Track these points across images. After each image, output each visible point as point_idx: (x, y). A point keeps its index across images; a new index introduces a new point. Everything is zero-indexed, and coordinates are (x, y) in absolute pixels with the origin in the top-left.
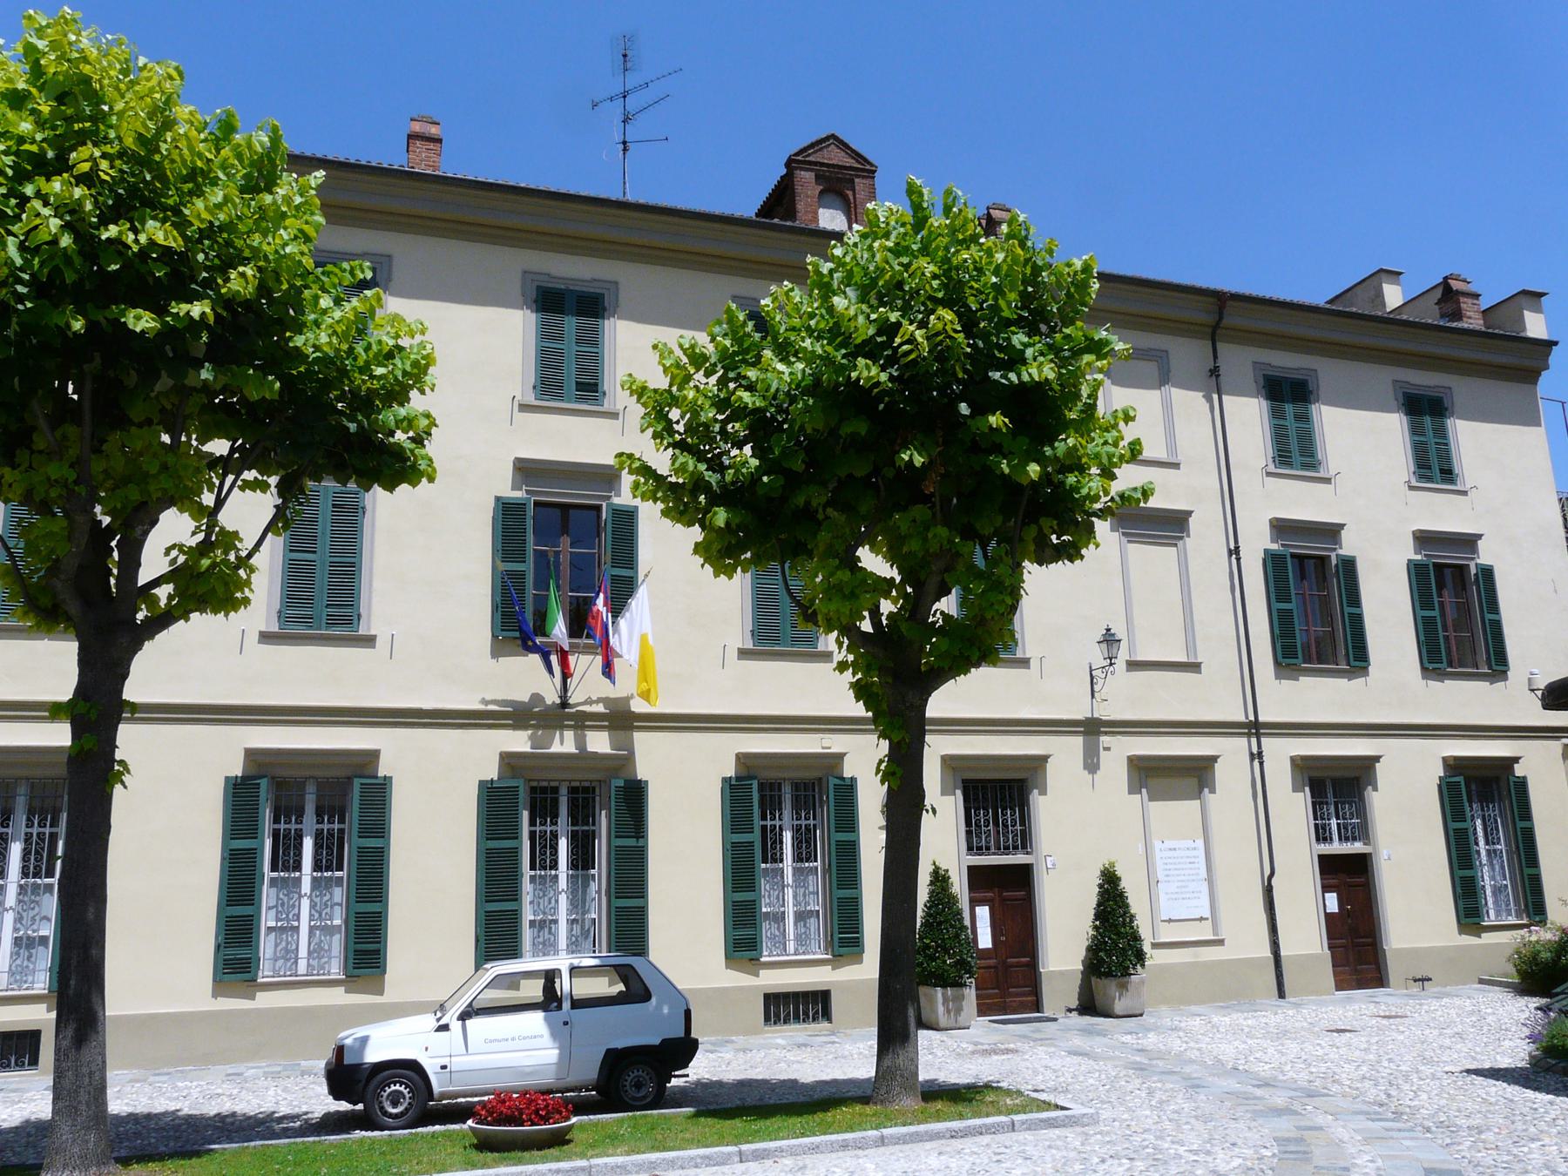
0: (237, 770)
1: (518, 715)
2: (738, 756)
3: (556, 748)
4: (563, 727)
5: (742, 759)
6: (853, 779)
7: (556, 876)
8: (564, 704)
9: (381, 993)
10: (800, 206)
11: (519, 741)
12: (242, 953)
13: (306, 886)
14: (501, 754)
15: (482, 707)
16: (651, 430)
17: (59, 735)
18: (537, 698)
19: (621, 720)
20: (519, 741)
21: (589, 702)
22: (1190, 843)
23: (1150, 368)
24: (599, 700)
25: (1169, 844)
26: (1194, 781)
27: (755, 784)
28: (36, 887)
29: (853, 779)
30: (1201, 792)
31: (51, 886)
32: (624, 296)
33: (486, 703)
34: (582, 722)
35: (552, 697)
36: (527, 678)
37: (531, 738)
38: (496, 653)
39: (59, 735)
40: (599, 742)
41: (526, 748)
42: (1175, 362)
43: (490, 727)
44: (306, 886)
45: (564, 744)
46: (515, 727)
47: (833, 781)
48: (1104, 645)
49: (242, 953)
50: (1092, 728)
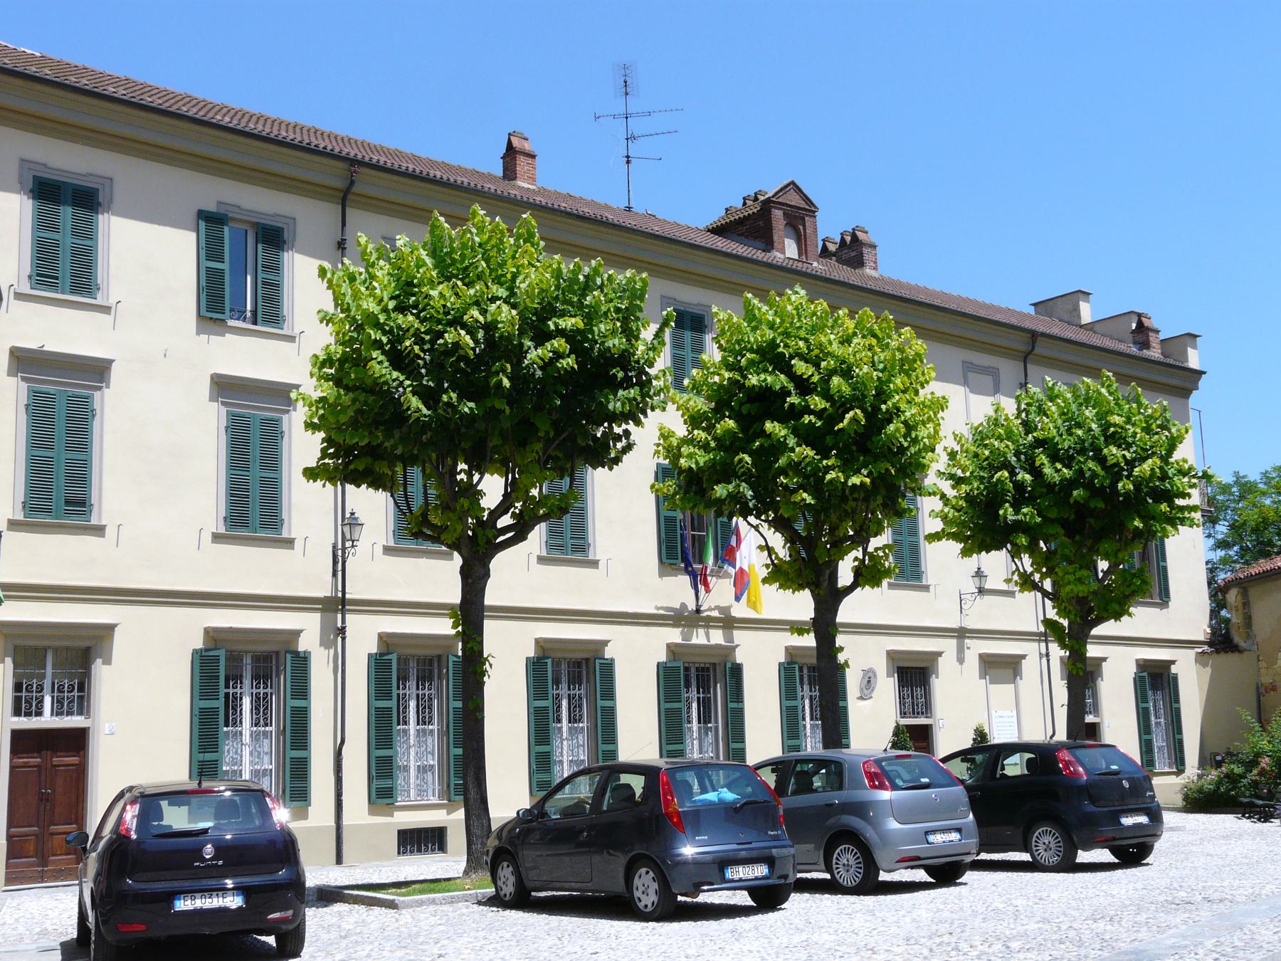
0: (199, 645)
1: (678, 618)
2: (787, 648)
3: (694, 641)
4: (698, 626)
5: (541, 644)
6: (612, 660)
7: (241, 733)
8: (698, 611)
9: (306, 818)
10: (775, 238)
11: (674, 635)
12: (385, 783)
13: (246, 738)
14: (205, 629)
15: (655, 612)
16: (957, 448)
17: (444, 627)
18: (683, 605)
19: (728, 623)
20: (674, 635)
21: (710, 609)
22: (1009, 713)
23: (988, 380)
24: (717, 608)
25: (1000, 713)
26: (1011, 672)
27: (549, 661)
28: (424, 730)
29: (612, 660)
30: (1015, 678)
31: (432, 731)
32: (301, 230)
33: (658, 609)
34: (709, 623)
35: (692, 606)
36: (678, 591)
37: (682, 633)
38: (661, 575)
39: (444, 627)
40: (717, 637)
41: (679, 640)
42: (1004, 377)
43: (661, 625)
44: (246, 738)
45: (699, 638)
46: (673, 626)
47: (729, 665)
48: (977, 579)
49: (385, 783)
50: (961, 634)
